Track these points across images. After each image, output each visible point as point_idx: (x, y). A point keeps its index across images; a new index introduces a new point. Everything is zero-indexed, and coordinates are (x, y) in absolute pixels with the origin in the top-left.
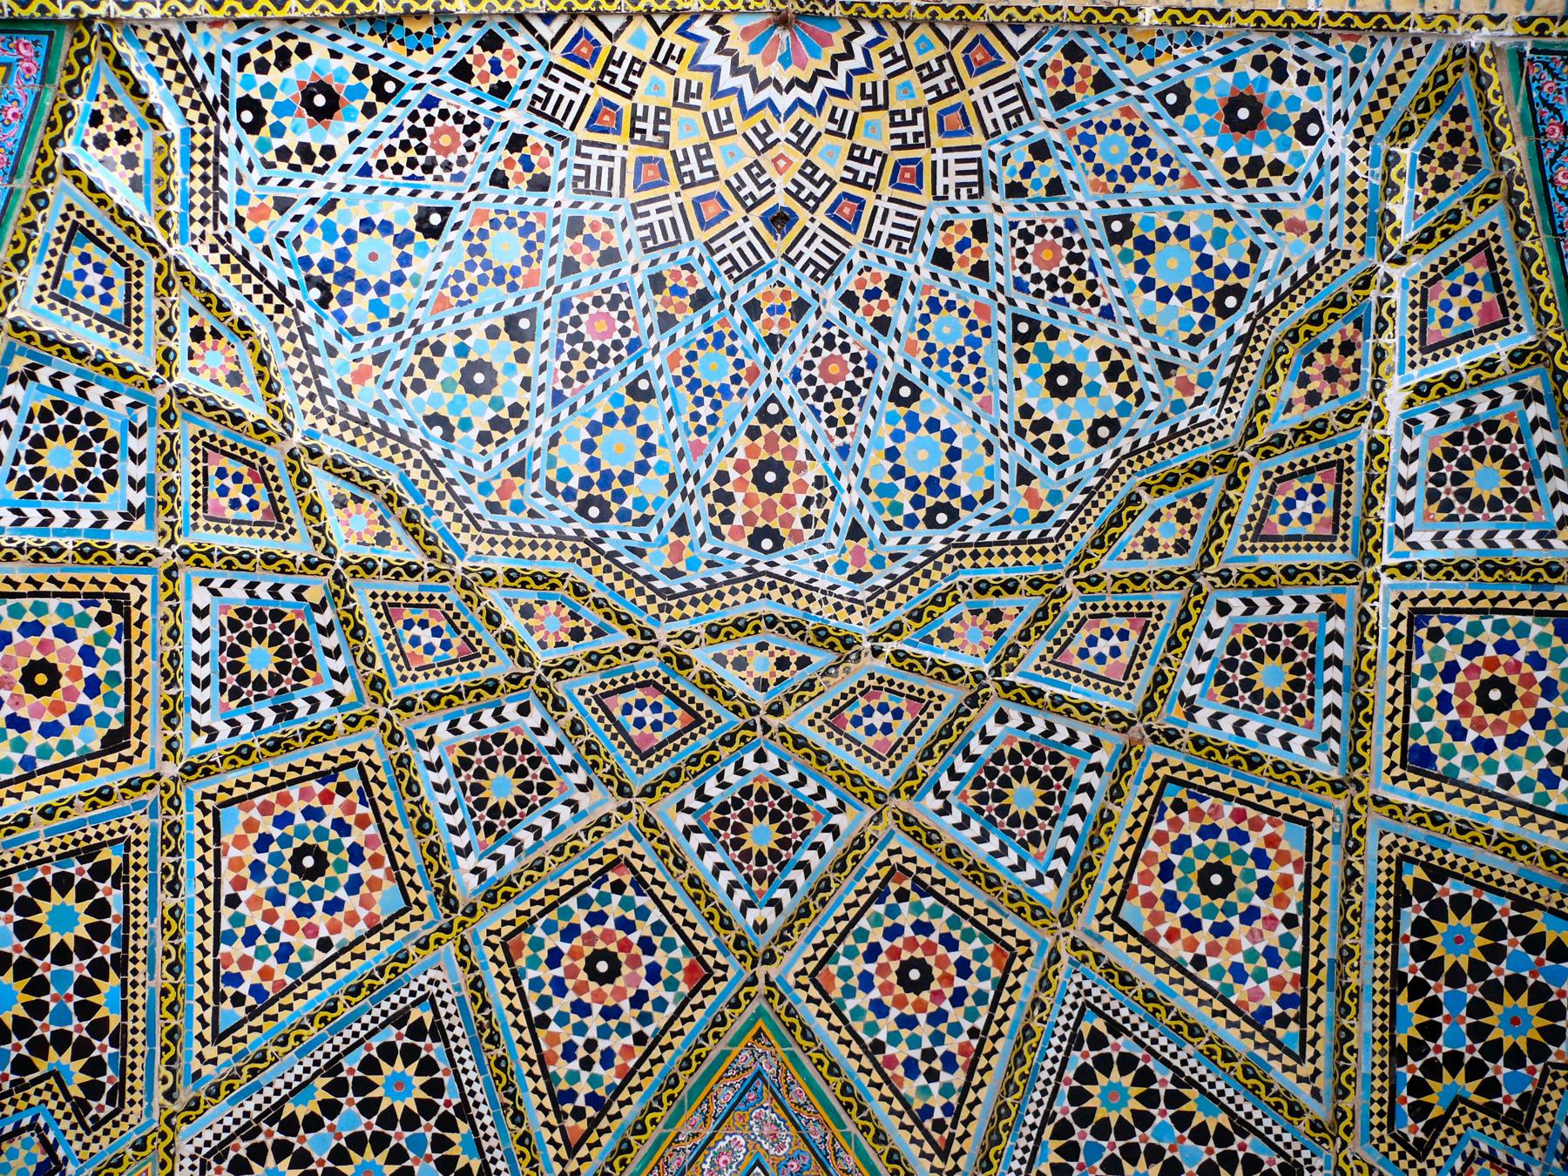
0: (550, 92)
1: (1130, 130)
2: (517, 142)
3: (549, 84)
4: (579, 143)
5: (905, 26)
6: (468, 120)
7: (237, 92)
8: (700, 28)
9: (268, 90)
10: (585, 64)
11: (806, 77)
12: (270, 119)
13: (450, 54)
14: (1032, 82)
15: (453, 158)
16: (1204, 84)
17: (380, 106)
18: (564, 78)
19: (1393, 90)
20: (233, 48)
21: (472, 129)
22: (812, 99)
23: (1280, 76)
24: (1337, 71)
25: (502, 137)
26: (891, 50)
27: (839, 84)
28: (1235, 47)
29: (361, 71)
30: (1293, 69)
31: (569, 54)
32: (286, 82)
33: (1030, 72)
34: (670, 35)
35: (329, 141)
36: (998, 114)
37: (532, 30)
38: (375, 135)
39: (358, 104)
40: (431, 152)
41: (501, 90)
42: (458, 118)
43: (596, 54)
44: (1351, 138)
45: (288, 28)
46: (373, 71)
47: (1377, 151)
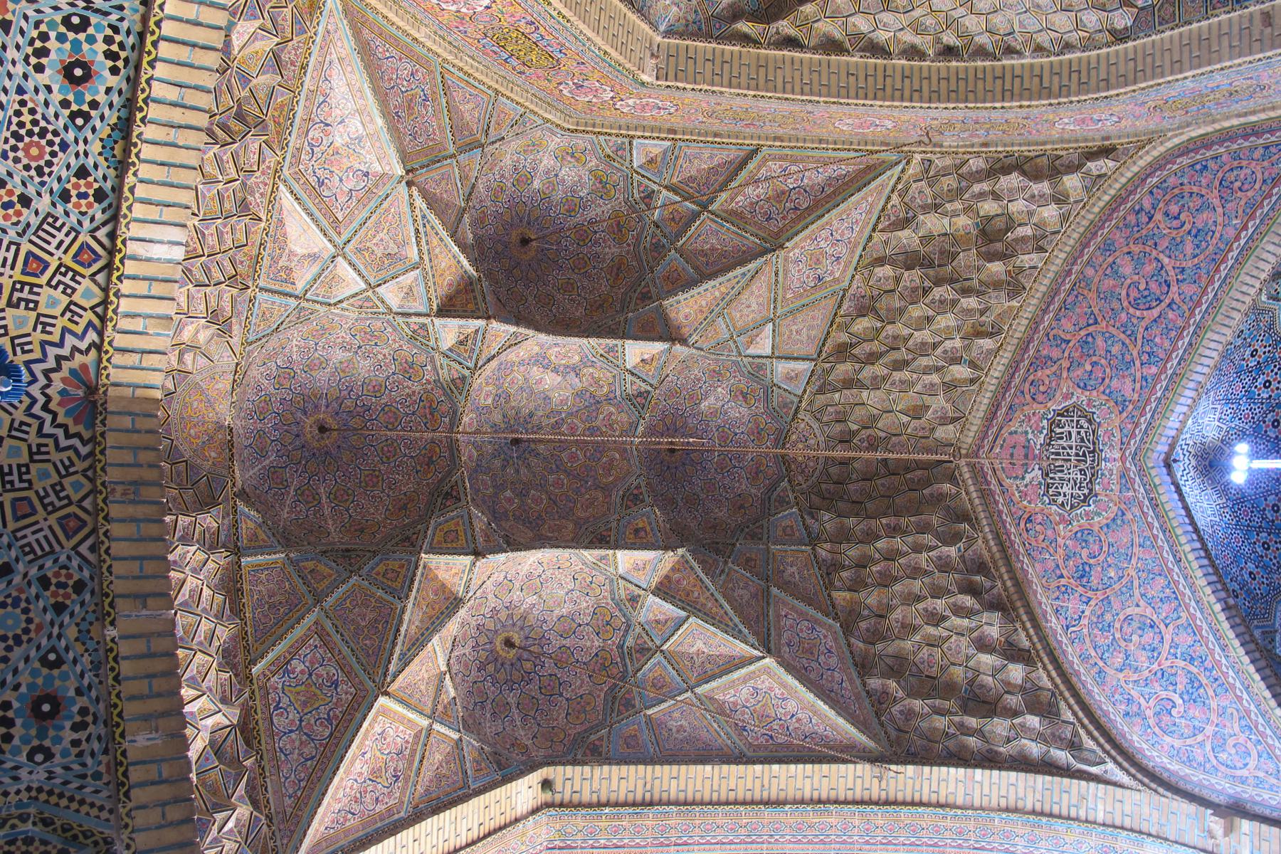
0: (59, 230)
1: (26, 631)
2: (25, 201)
3: (65, 230)
4: (18, 245)
5: (90, 473)
6: (47, 170)
7: (94, 19)
8: (92, 336)
9: (91, 40)
10: (75, 256)
11: (52, 406)
12: (71, 35)
13: (96, 166)
14: (56, 561)
15: (20, 154)
16: (65, 677)
17: (67, 112)
18: (68, 241)
19: (74, 805)
20: (125, 25)
21: (40, 171)
22: (37, 410)
23: (75, 728)
24: (84, 765)
25: (31, 191)
26: (72, 464)
27: (47, 429)
28: (94, 694)
29: (94, 105)
30: (82, 735)
31: (85, 247)
32: (96, 52)
33: (63, 558)
34: (89, 316)
35: (48, 71)
36: (31, 539)
37: (104, 224)
38: (47, 104)
39: (71, 97)
40: (27, 139)
41: (65, 196)
42: (49, 164)
43: (82, 264)
44: (35, 785)
45: (131, 64)
46: (93, 113)
47: (28, 806)
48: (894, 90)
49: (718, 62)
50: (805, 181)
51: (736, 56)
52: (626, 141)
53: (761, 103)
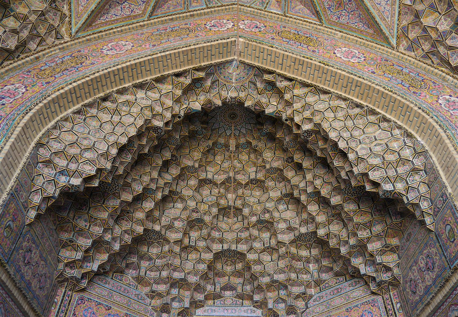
48: (128, 72)
49: (209, 56)
50: (119, 8)
51: (202, 61)
52: (209, 6)
53: (183, 43)
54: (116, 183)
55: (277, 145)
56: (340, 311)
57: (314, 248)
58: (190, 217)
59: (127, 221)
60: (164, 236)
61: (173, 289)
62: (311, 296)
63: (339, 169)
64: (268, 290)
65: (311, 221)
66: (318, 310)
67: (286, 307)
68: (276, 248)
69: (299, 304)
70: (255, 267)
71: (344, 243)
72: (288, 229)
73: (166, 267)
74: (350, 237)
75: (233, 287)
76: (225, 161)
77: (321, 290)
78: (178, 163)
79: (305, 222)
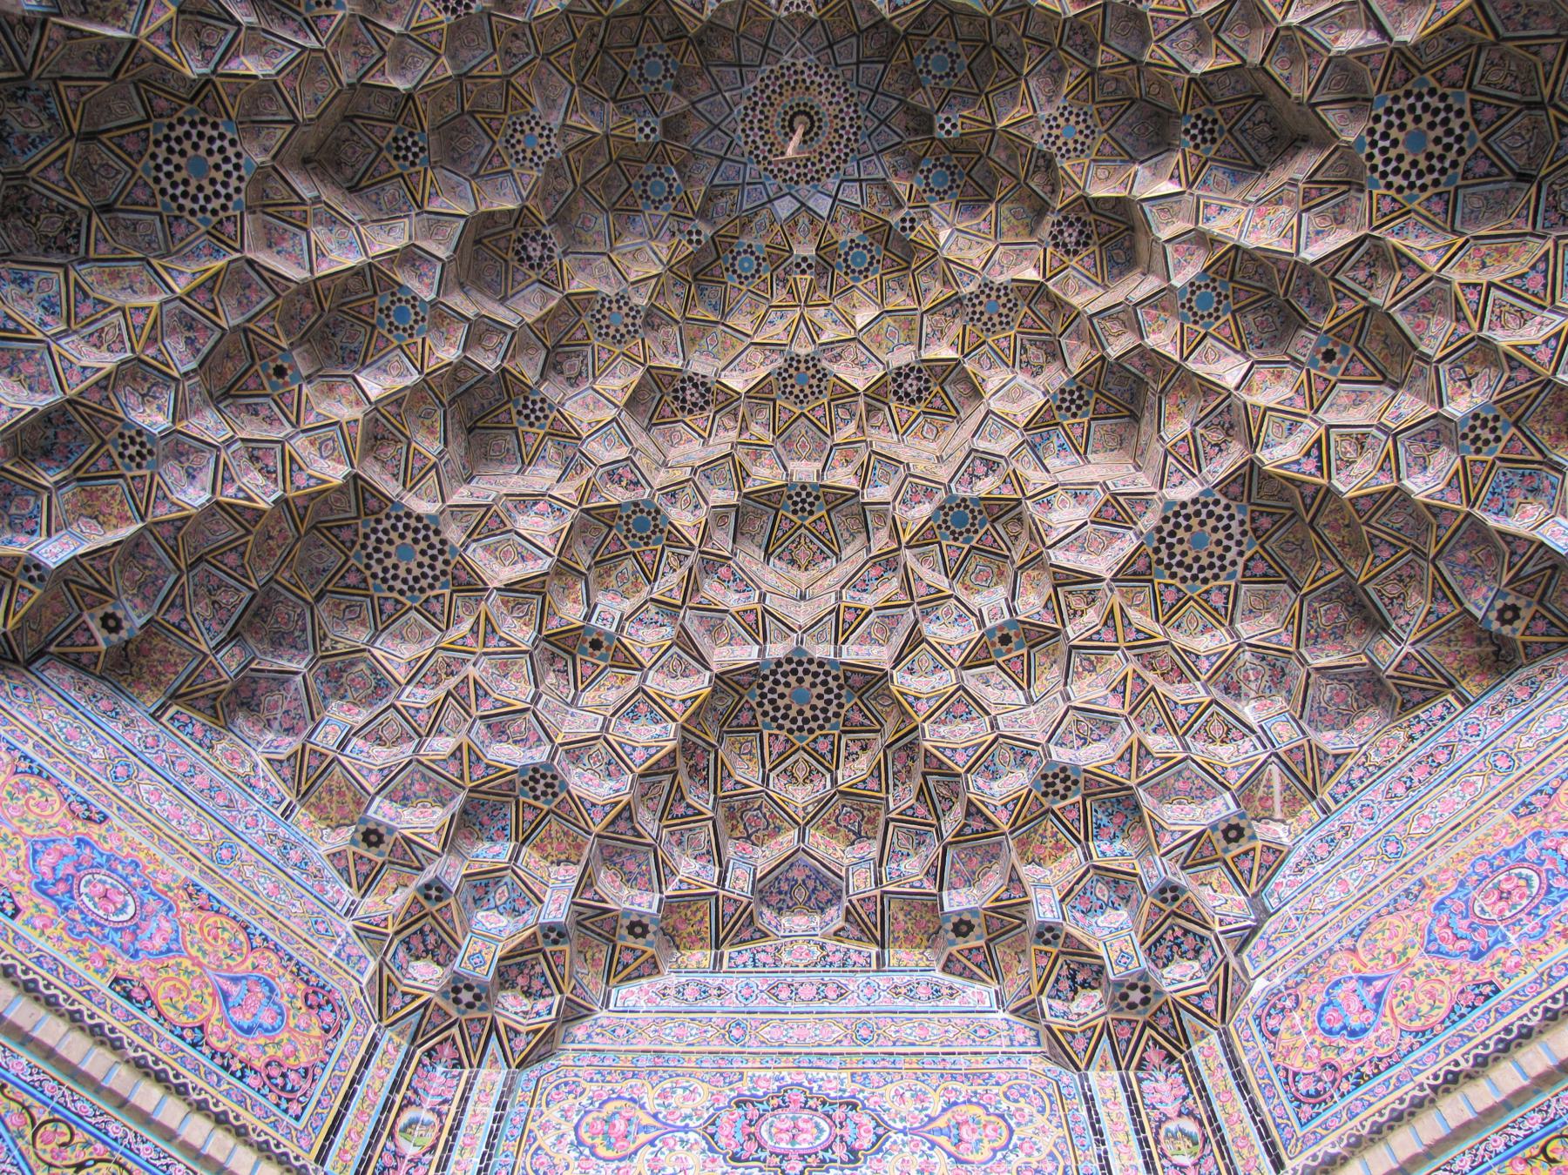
54: (231, 152)
55: (1004, 209)
56: (1480, 834)
57: (1252, 612)
58: (595, 490)
59: (270, 420)
60: (454, 550)
61: (487, 845)
62: (1277, 855)
63: (1317, 32)
64: (1023, 844)
65: (1216, 436)
66: (1334, 893)
67: (1134, 918)
68: (1049, 621)
69: (1214, 898)
70: (943, 730)
71: (1418, 449)
72: (1098, 519)
73: (452, 714)
74: (1448, 389)
75: (825, 883)
76: (772, 316)
77: (1325, 810)
78: (552, 275)
79: (1191, 457)
